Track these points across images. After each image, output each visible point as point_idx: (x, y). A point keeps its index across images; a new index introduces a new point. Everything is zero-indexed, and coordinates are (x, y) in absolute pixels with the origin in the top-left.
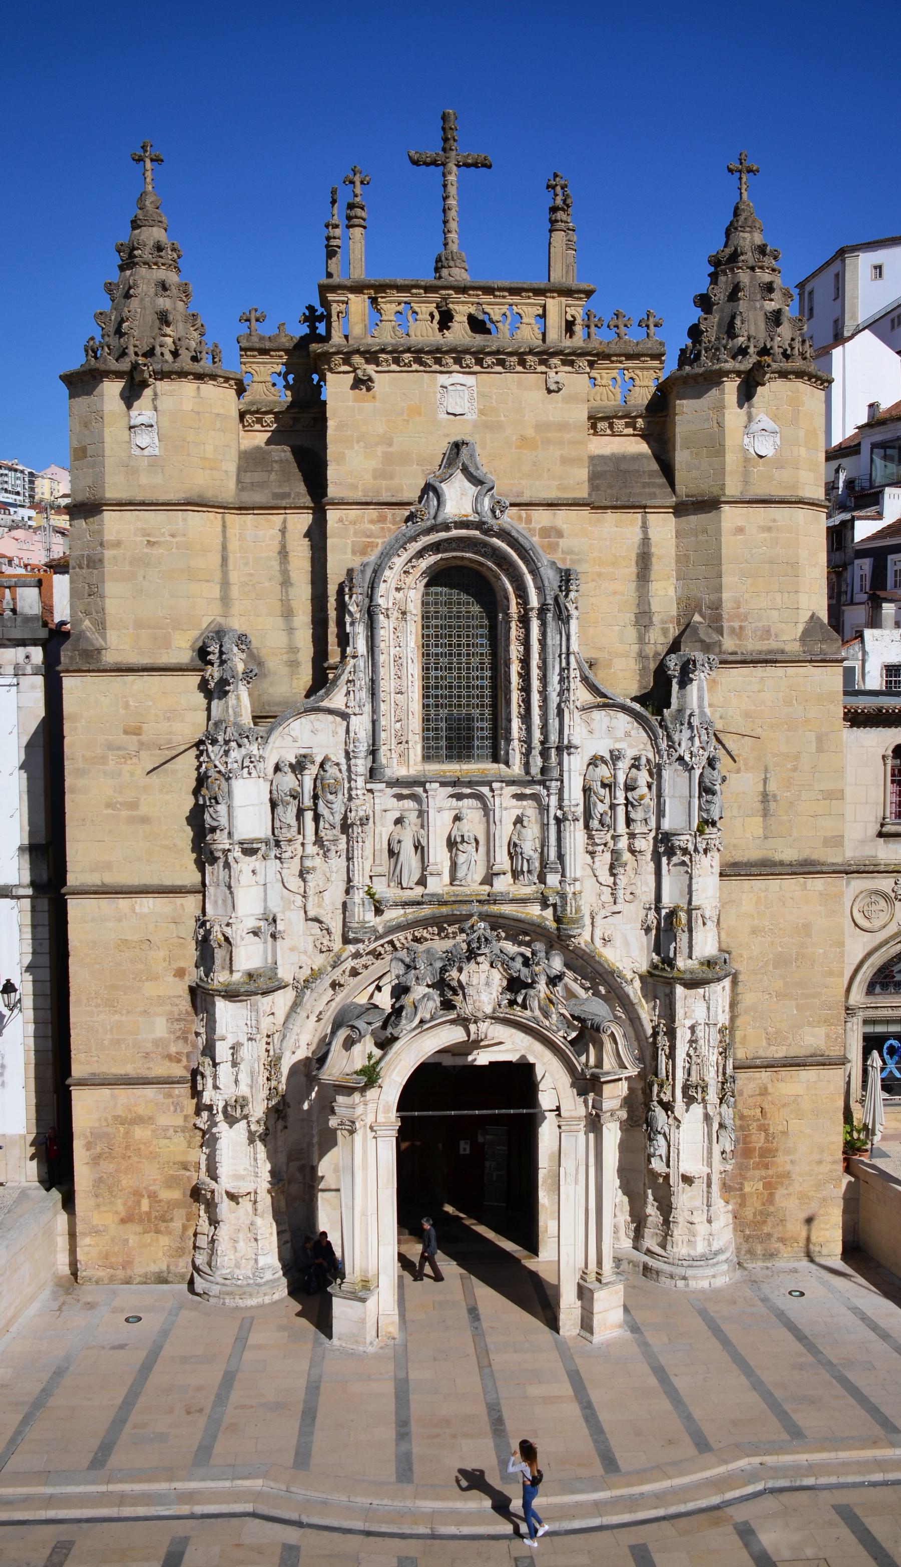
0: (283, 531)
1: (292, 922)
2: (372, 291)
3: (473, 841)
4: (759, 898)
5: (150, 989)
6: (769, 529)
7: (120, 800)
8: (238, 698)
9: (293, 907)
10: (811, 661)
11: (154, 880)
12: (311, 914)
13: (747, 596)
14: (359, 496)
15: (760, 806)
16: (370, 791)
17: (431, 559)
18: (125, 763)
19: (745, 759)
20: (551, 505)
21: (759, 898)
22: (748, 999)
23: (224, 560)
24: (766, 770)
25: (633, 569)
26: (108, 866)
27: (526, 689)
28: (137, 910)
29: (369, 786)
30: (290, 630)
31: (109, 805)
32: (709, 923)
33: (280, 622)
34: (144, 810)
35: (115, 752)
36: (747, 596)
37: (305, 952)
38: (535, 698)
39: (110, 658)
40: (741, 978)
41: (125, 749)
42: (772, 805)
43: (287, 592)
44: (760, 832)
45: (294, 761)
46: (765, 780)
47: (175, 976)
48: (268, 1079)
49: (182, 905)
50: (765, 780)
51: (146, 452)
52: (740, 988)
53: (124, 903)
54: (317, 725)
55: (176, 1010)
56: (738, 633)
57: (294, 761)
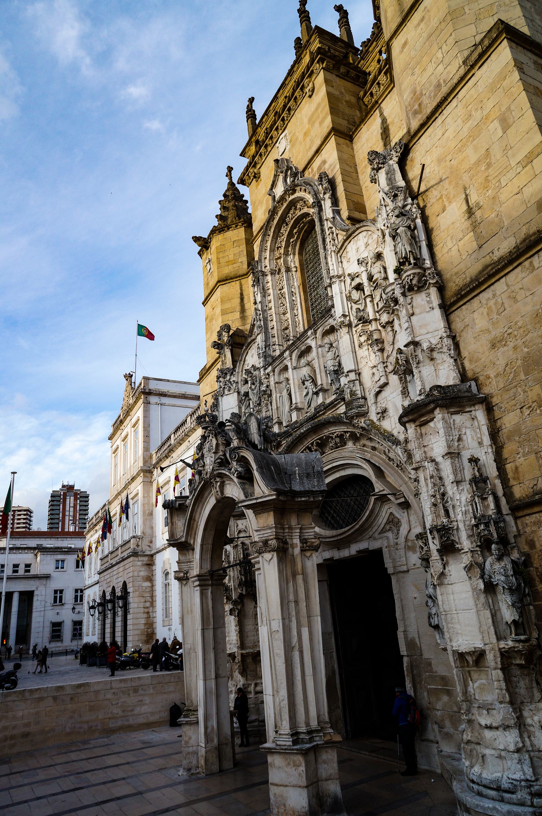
3: (308, 378)
4: (490, 309)
8: (225, 356)
10: (472, 67)
15: (467, 224)
16: (268, 374)
17: (285, 231)
19: (446, 195)
21: (490, 309)
22: (508, 421)
23: (242, 299)
24: (465, 189)
29: (267, 371)
32: (435, 354)
36: (418, 79)
40: (495, 400)
52: (497, 413)
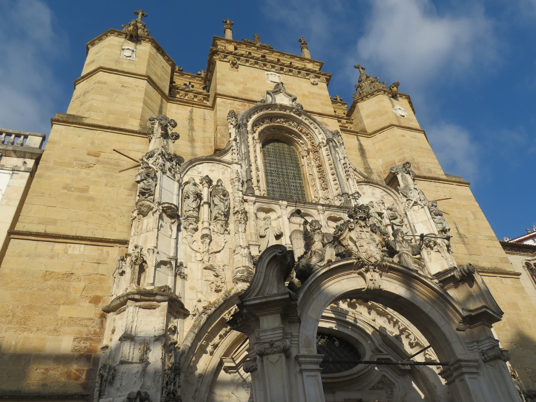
0: (191, 112)
1: (194, 269)
2: (235, 44)
5: (64, 312)
6: (415, 138)
7: (75, 186)
9: (193, 260)
11: (90, 235)
12: (207, 264)
13: (415, 157)
14: (233, 95)
16: (246, 201)
18: (85, 169)
20: (320, 114)
24: (455, 224)
25: (358, 153)
26: (54, 222)
27: (323, 177)
28: (70, 251)
29: (245, 197)
30: (193, 147)
31: (65, 188)
33: (188, 143)
34: (91, 193)
35: (78, 162)
37: (201, 292)
38: (330, 178)
39: (86, 121)
41: (86, 162)
42: (466, 240)
43: (192, 133)
44: (466, 252)
45: (198, 181)
46: (457, 228)
47: (90, 302)
48: (167, 383)
49: (108, 252)
50: (457, 228)
51: (128, 58)
53: (59, 247)
54: (213, 168)
55: (85, 330)
56: (418, 168)
57: (198, 181)
